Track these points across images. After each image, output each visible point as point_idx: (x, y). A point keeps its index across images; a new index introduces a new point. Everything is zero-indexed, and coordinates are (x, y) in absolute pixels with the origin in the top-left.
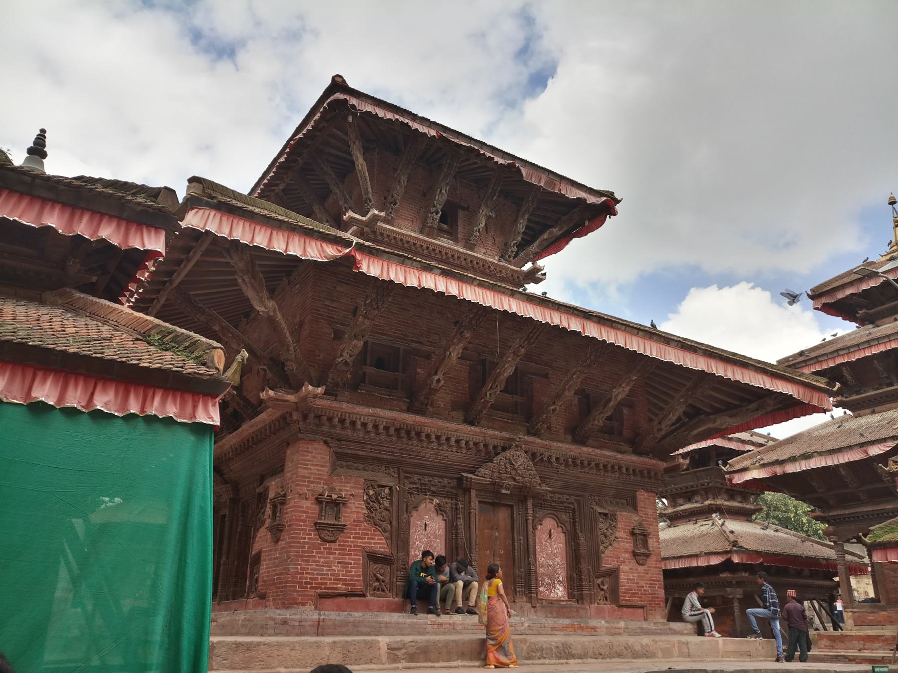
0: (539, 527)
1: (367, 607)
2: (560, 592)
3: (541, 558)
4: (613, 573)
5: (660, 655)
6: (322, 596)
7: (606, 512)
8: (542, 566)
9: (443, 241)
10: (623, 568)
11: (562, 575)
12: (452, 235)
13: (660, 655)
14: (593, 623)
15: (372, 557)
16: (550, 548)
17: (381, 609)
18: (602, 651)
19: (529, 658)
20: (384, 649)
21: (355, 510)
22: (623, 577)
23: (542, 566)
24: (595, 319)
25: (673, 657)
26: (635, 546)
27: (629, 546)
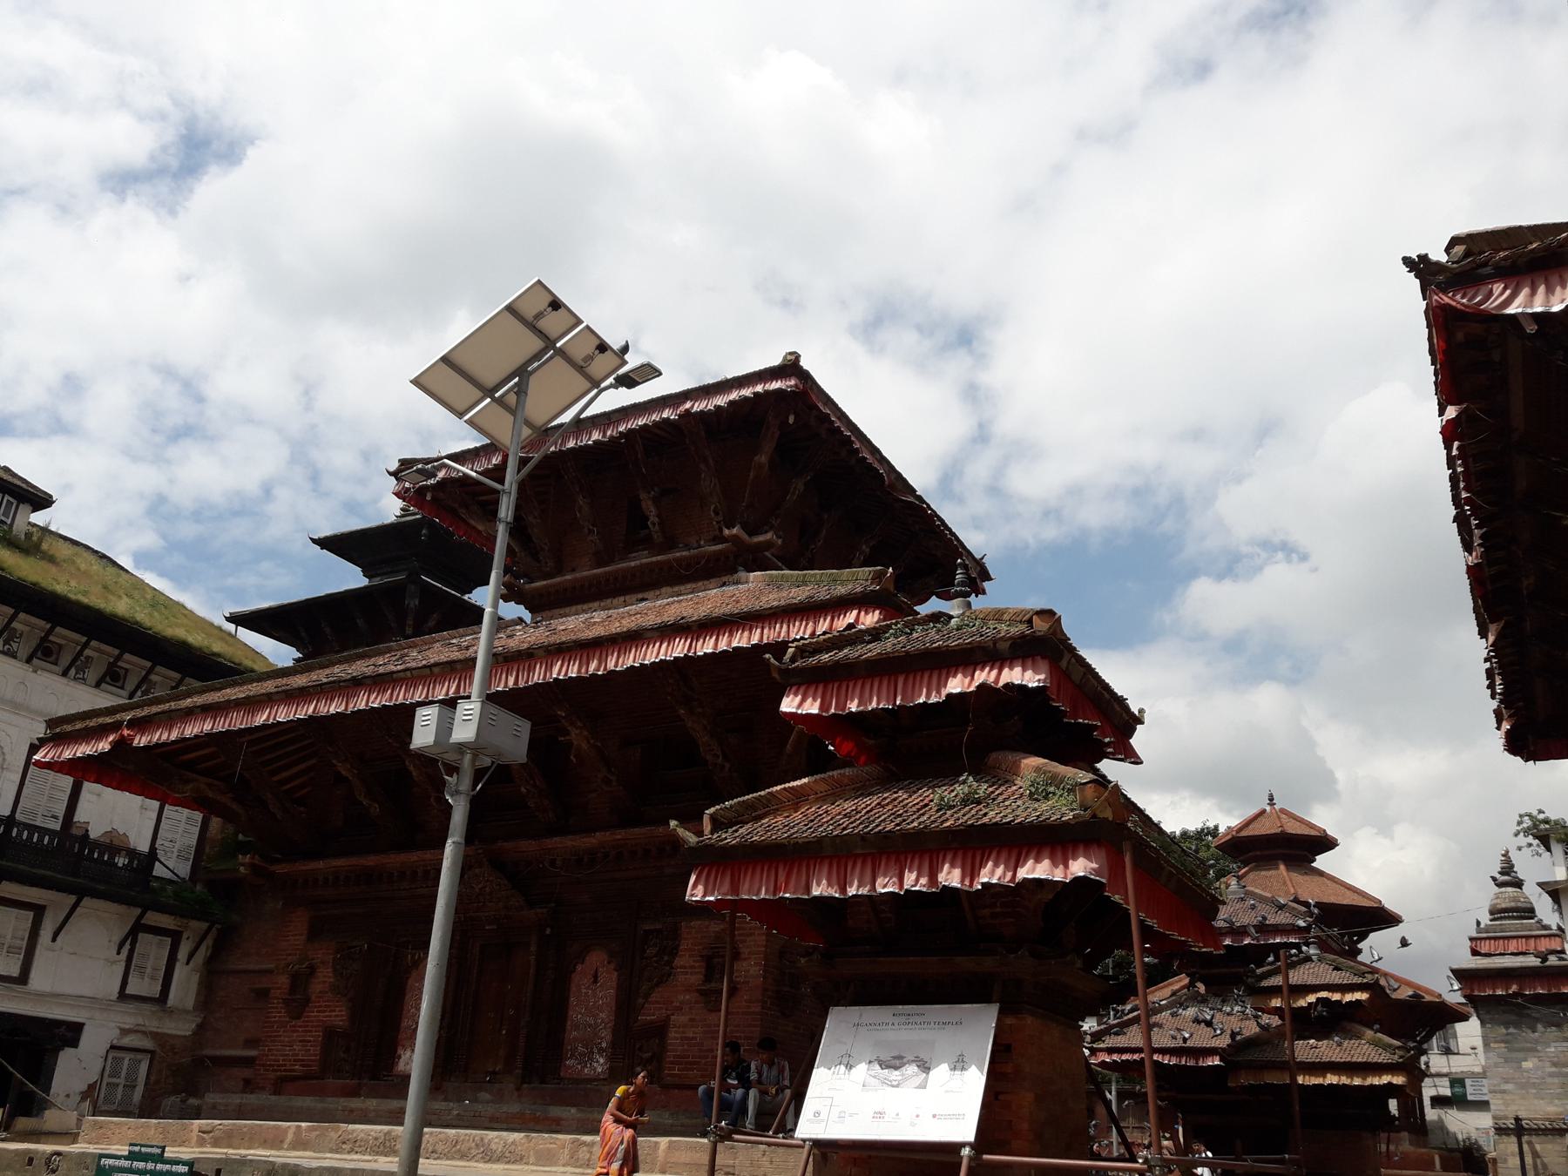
0: (579, 968)
1: (321, 1093)
2: (600, 1065)
3: (576, 1014)
4: (659, 1030)
5: (532, 1160)
6: (284, 1080)
7: (658, 926)
8: (577, 1027)
9: (635, 559)
10: (679, 1019)
11: (605, 1037)
12: (647, 543)
13: (532, 1160)
14: (556, 1111)
15: (330, 1034)
16: (593, 1000)
17: (334, 1094)
18: (440, 1148)
19: (337, 1152)
20: (196, 1132)
21: (325, 977)
22: (673, 1035)
23: (577, 1027)
24: (369, 681)
25: (555, 1164)
26: (708, 978)
27: (696, 979)
